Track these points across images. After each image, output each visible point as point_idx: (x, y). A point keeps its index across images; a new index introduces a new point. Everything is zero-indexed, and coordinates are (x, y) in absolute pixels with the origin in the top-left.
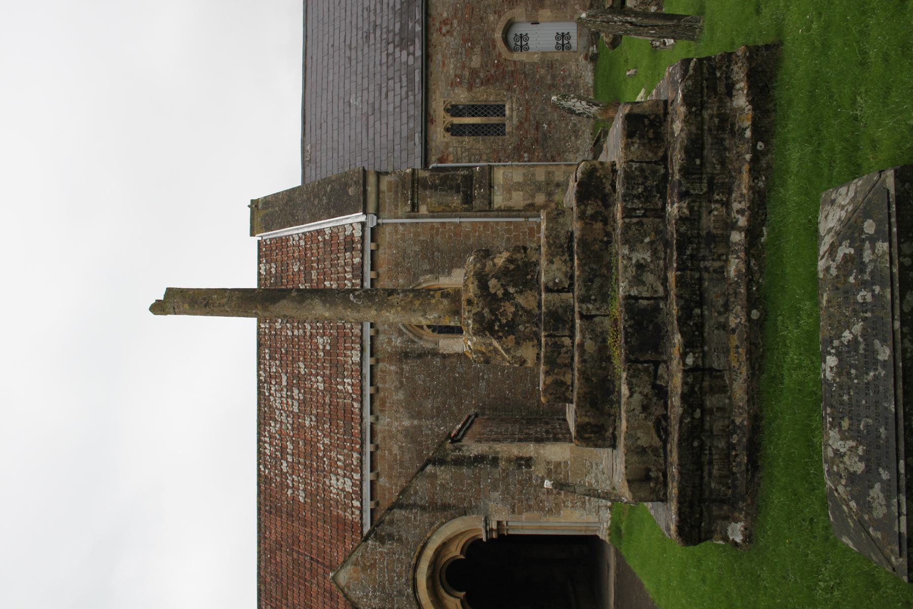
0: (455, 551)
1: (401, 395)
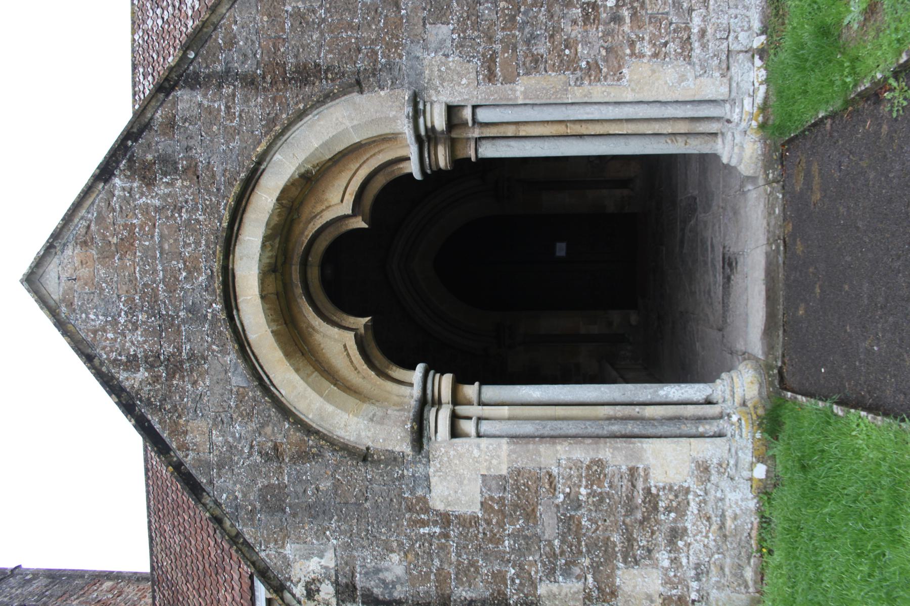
0: (337, 202)
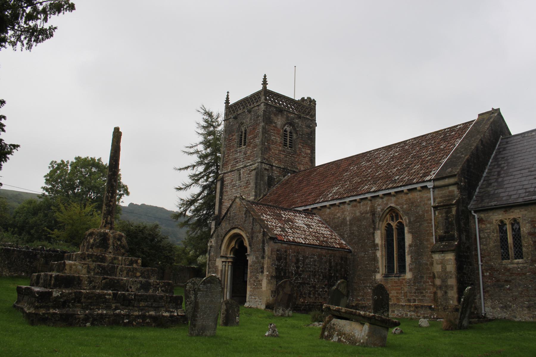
1: (358, 214)
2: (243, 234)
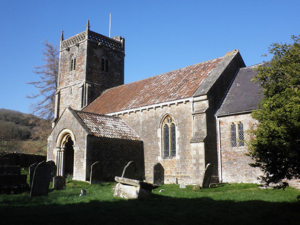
1: (147, 118)
2: (70, 132)
